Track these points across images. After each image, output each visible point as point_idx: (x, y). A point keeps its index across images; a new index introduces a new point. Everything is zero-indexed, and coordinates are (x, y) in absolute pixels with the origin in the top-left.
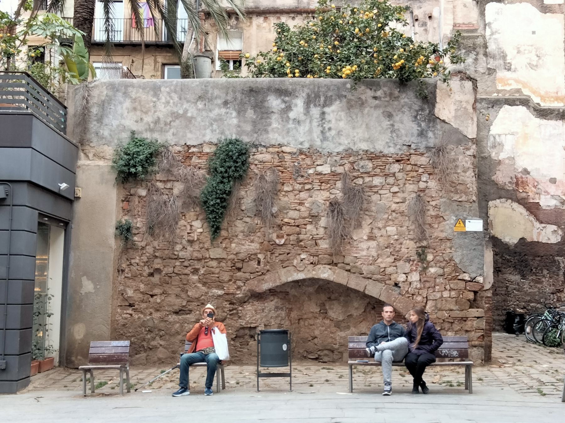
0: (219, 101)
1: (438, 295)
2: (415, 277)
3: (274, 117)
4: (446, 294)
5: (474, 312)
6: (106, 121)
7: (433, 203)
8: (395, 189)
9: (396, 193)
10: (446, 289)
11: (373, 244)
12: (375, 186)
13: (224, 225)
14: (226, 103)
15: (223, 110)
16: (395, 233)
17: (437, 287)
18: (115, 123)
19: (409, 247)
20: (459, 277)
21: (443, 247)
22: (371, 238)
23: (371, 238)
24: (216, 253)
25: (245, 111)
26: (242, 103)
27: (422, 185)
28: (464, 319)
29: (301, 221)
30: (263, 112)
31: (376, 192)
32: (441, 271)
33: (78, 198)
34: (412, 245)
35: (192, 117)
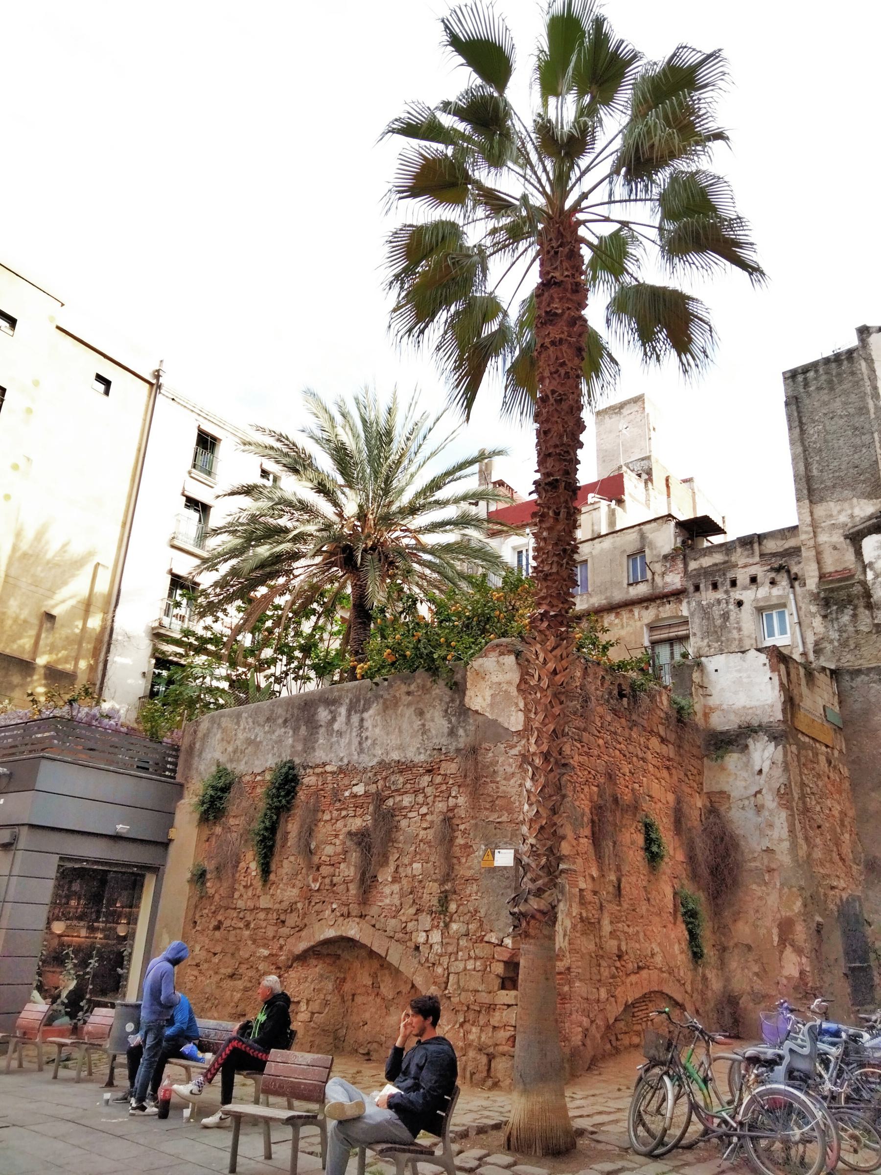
0: (280, 721)
1: (461, 966)
2: (436, 937)
3: (322, 731)
4: (470, 965)
5: (506, 996)
6: (204, 755)
7: (462, 827)
8: (424, 810)
9: (425, 814)
10: (470, 958)
11: (396, 887)
12: (405, 808)
13: (273, 867)
14: (285, 721)
15: (283, 730)
16: (420, 871)
17: (460, 953)
18: (209, 756)
19: (431, 891)
20: (486, 939)
21: (468, 892)
22: (396, 880)
23: (396, 880)
24: (264, 902)
25: (299, 728)
26: (298, 720)
27: (452, 802)
28: (491, 1008)
29: (335, 859)
30: (312, 725)
31: (405, 816)
32: (463, 930)
33: (171, 840)
34: (434, 887)
35: (261, 742)
